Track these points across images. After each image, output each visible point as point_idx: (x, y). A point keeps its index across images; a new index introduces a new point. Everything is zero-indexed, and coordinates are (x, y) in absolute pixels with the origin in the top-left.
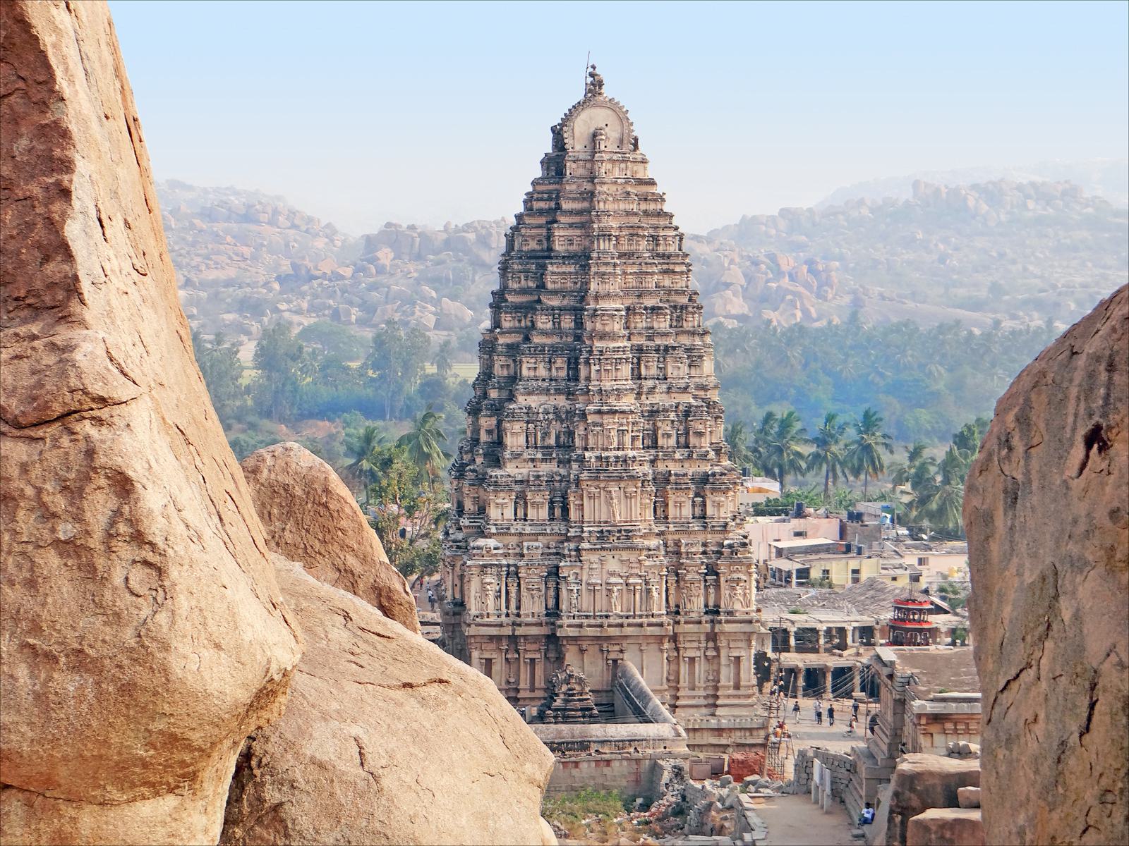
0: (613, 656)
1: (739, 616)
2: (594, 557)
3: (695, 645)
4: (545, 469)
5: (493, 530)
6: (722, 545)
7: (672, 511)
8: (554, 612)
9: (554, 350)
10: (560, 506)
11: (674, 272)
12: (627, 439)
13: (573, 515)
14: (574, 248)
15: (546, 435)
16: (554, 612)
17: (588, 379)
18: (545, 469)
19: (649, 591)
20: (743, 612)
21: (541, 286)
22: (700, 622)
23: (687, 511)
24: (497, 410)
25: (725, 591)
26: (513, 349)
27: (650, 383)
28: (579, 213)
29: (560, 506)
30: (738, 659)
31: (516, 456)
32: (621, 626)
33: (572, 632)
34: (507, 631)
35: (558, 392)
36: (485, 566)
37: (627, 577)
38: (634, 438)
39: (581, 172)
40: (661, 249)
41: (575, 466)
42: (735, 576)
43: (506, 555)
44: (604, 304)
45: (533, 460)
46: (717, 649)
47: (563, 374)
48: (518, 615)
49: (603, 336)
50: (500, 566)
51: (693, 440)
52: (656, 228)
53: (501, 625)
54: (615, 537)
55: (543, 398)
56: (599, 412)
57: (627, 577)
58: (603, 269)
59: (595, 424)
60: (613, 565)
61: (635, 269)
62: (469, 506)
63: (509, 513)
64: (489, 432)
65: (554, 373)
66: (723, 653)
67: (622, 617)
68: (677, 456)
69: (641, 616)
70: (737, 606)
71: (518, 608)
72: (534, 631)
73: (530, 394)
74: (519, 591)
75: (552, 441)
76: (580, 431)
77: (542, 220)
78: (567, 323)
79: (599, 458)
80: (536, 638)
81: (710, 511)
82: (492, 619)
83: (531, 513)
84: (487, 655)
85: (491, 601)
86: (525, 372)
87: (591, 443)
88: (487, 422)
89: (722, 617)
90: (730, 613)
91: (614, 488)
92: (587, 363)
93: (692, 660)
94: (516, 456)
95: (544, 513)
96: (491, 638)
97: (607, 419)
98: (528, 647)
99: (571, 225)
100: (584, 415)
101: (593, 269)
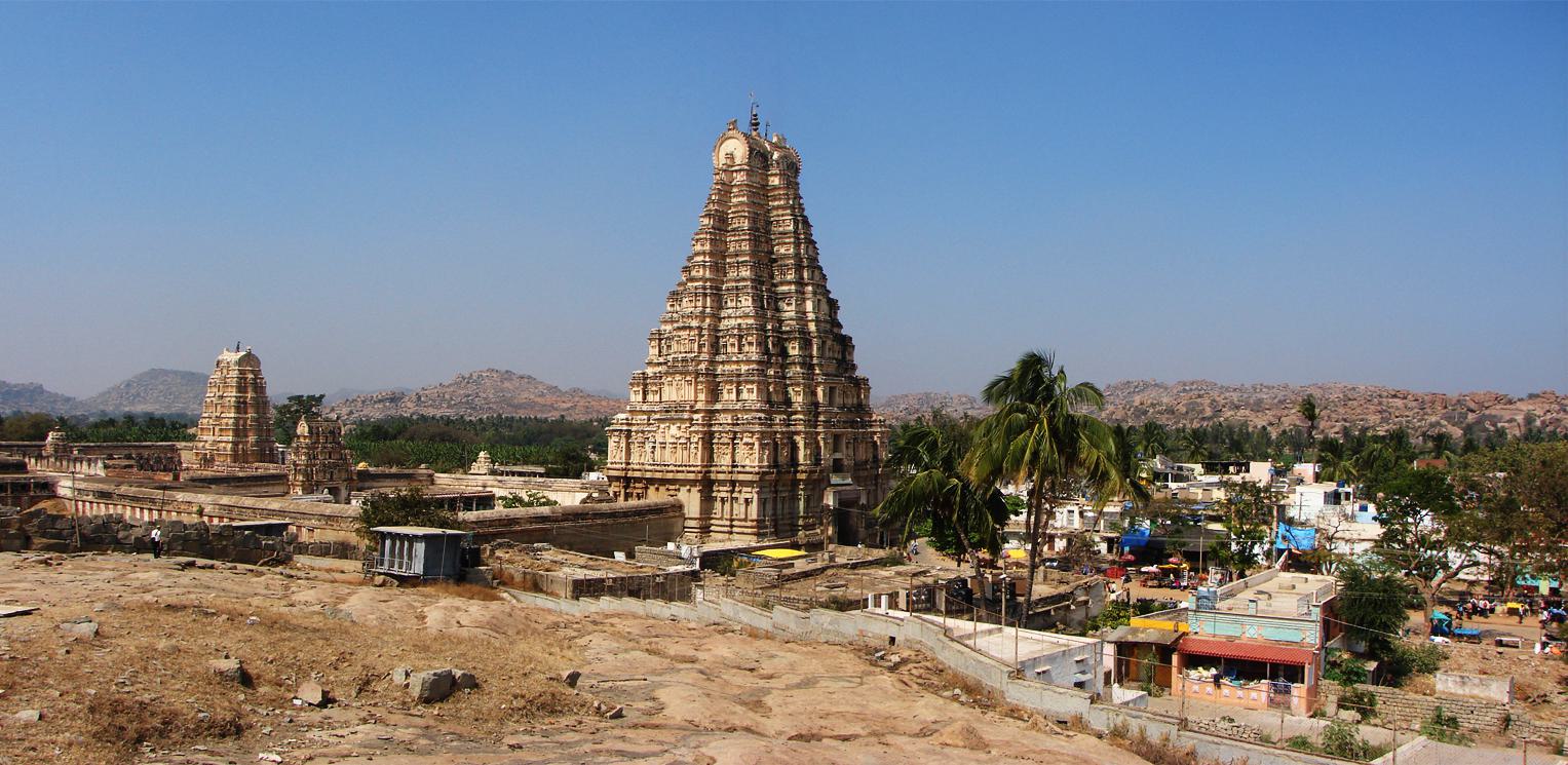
1: (748, 469)
3: (725, 488)
11: (786, 243)
20: (751, 467)
23: (733, 396)
27: (730, 311)
34: (623, 474)
37: (680, 438)
38: (700, 346)
40: (781, 229)
43: (628, 424)
52: (779, 216)
56: (679, 329)
57: (680, 438)
61: (737, 238)
67: (675, 466)
68: (734, 359)
69: (686, 466)
70: (747, 462)
90: (743, 467)
91: (678, 377)
93: (722, 499)
98: (637, 485)
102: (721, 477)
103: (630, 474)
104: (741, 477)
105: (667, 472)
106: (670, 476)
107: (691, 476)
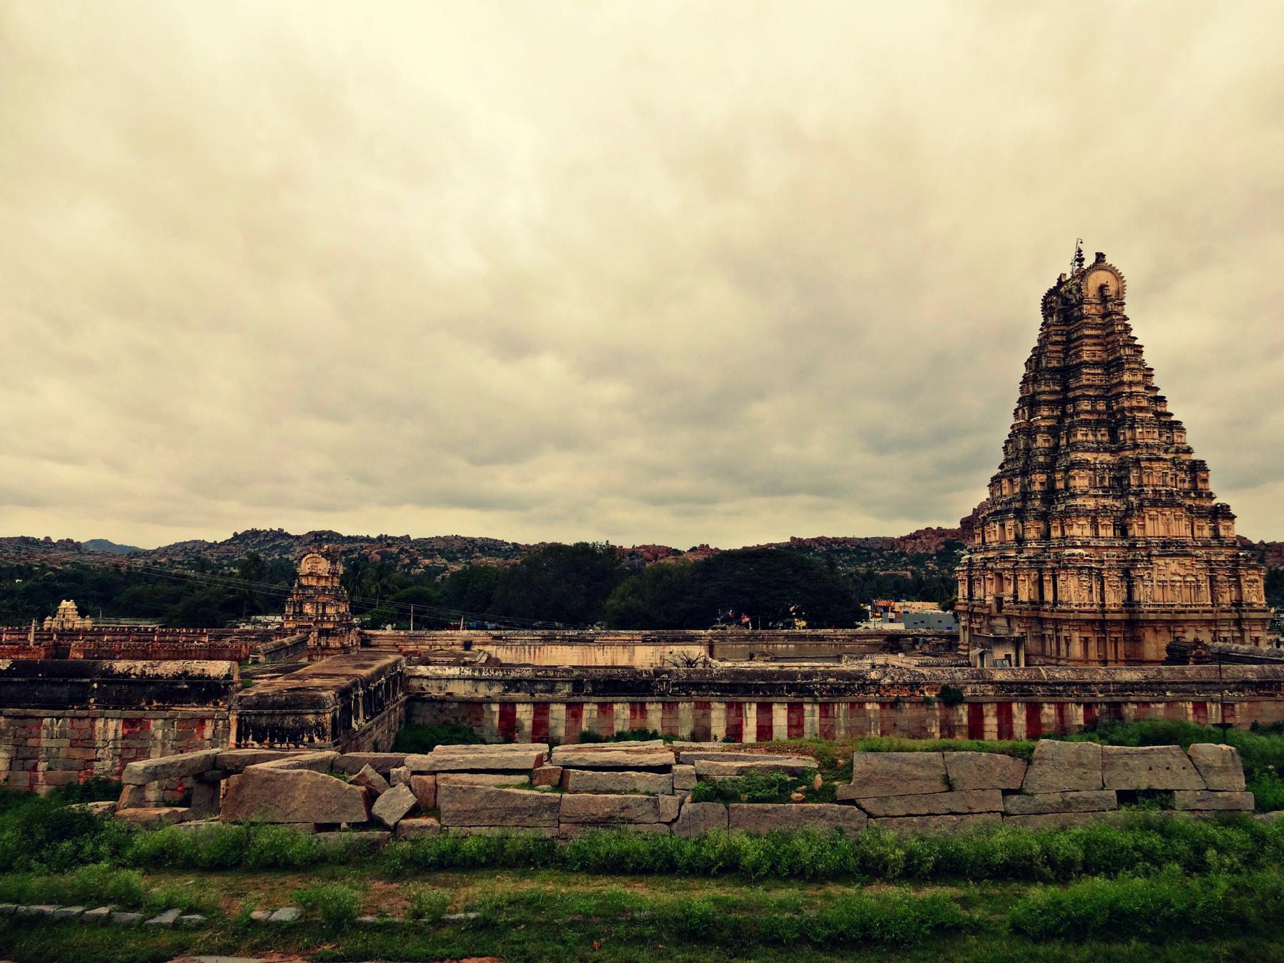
0: (1178, 634)
2: (1161, 562)
4: (1108, 502)
5: (1079, 543)
6: (1238, 556)
7: (1197, 533)
8: (1130, 602)
9: (1099, 423)
10: (1122, 530)
12: (1168, 479)
13: (1135, 531)
14: (1096, 359)
15: (1102, 479)
16: (1130, 602)
17: (1133, 439)
18: (1108, 502)
19: (1199, 587)
21: (1066, 389)
22: (1230, 611)
23: (1207, 533)
24: (1050, 468)
25: (1246, 590)
26: (1053, 432)
28: (1097, 337)
29: (1122, 530)
30: (1257, 638)
31: (1085, 493)
32: (1183, 612)
33: (1152, 616)
34: (1100, 616)
35: (1106, 450)
36: (1081, 568)
39: (1093, 311)
41: (1132, 499)
42: (1253, 577)
44: (1134, 389)
45: (1095, 496)
46: (1242, 631)
47: (1106, 438)
48: (1104, 605)
49: (1141, 409)
50: (1090, 568)
51: (1200, 485)
53: (1095, 612)
54: (1171, 547)
55: (1095, 455)
56: (1149, 460)
58: (1132, 366)
59: (1146, 468)
60: (1174, 566)
62: (1032, 534)
63: (1088, 532)
64: (1042, 484)
65: (1099, 438)
66: (1247, 635)
70: (1254, 600)
71: (1103, 599)
72: (1118, 617)
73: (1086, 451)
74: (1102, 588)
75: (1106, 484)
76: (1134, 473)
77: (1059, 348)
78: (1101, 406)
79: (1155, 491)
80: (1117, 622)
81: (1222, 533)
82: (1087, 608)
83: (1102, 532)
84: (1085, 635)
85: (1085, 594)
86: (1079, 437)
87: (1145, 481)
88: (1039, 478)
89: (1245, 607)
90: (1250, 604)
92: (1132, 428)
94: (1085, 493)
95: (1110, 533)
96: (1088, 622)
97: (1155, 465)
99: (1095, 344)
100: (1138, 461)
101: (1127, 366)
102: (1227, 615)
103: (1108, 616)
104: (1253, 615)
105: (1177, 612)
106: (1182, 617)
107: (1209, 616)
